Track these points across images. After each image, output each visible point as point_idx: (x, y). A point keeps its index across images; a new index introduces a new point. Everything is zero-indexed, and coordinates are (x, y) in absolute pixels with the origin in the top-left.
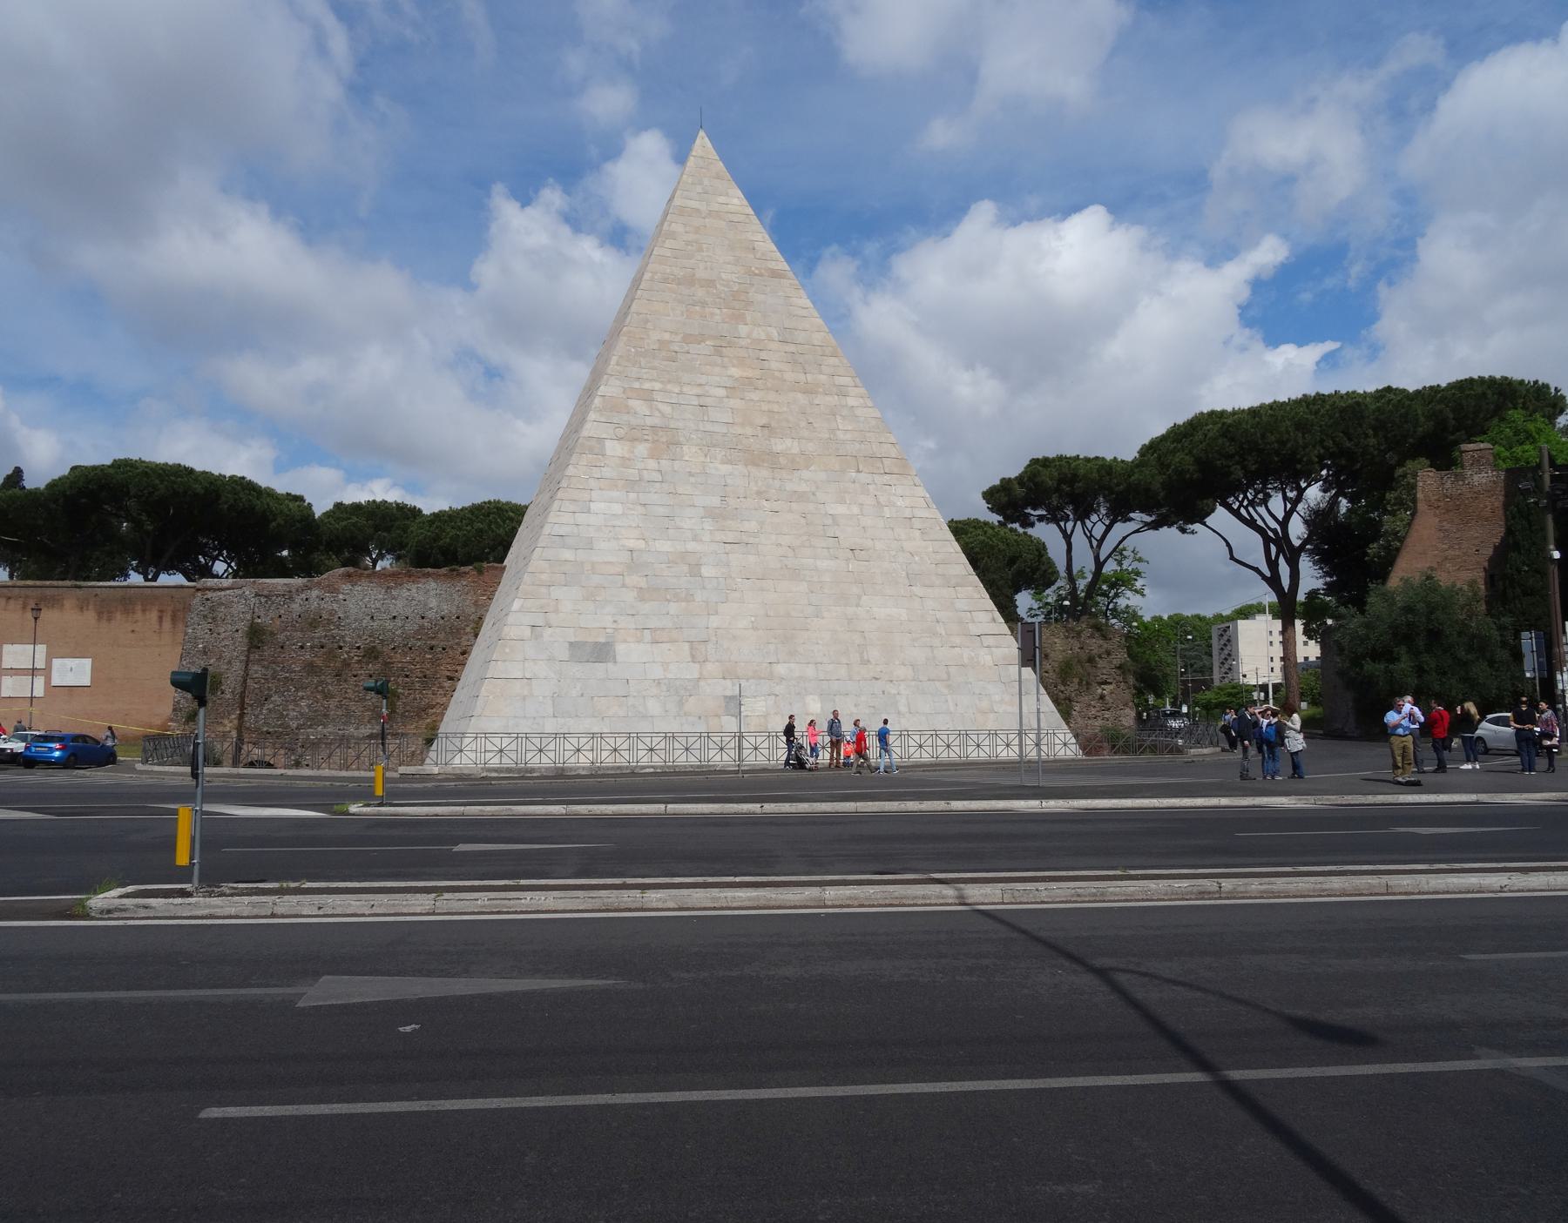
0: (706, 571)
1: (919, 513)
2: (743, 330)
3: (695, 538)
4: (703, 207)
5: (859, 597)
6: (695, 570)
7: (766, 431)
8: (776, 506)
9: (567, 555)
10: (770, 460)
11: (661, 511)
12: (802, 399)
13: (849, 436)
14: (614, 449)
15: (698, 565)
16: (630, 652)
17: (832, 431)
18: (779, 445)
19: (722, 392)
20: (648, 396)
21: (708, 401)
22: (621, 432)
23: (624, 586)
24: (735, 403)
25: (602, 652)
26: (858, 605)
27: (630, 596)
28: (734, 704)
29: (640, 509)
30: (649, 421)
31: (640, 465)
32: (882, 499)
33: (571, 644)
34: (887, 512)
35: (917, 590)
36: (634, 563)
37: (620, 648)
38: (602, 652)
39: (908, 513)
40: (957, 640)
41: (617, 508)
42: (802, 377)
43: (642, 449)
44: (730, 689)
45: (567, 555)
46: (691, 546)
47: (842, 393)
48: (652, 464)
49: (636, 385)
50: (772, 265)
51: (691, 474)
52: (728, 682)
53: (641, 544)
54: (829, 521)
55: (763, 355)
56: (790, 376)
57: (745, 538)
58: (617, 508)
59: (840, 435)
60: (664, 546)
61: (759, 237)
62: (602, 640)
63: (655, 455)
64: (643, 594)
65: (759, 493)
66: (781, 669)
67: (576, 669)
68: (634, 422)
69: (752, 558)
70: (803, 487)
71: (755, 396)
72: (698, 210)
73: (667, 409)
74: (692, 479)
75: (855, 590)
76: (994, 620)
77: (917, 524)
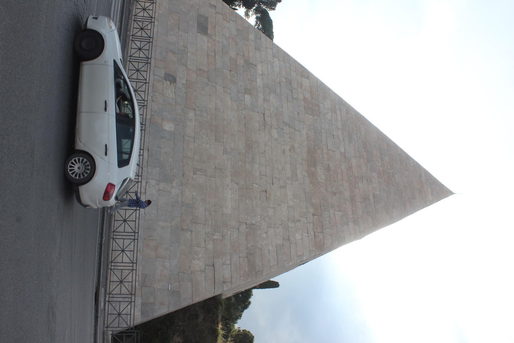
0: (248, 98)
3: (265, 100)
5: (237, 184)
6: (247, 91)
11: (278, 90)
12: (347, 194)
13: (332, 216)
15: (250, 94)
16: (203, 41)
18: (320, 171)
19: (342, 150)
23: (238, 54)
25: (203, 28)
26: (232, 181)
27: (232, 53)
28: (171, 78)
29: (278, 80)
30: (321, 105)
33: (207, 18)
34: (291, 225)
35: (243, 228)
36: (249, 65)
37: (205, 38)
38: (203, 28)
40: (210, 246)
41: (277, 70)
43: (308, 95)
44: (181, 81)
46: (261, 96)
48: (301, 97)
49: (337, 107)
51: (298, 114)
52: (184, 82)
55: (365, 181)
58: (277, 70)
59: (332, 211)
60: (259, 82)
62: (209, 32)
66: (191, 114)
70: (300, 176)
74: (296, 113)
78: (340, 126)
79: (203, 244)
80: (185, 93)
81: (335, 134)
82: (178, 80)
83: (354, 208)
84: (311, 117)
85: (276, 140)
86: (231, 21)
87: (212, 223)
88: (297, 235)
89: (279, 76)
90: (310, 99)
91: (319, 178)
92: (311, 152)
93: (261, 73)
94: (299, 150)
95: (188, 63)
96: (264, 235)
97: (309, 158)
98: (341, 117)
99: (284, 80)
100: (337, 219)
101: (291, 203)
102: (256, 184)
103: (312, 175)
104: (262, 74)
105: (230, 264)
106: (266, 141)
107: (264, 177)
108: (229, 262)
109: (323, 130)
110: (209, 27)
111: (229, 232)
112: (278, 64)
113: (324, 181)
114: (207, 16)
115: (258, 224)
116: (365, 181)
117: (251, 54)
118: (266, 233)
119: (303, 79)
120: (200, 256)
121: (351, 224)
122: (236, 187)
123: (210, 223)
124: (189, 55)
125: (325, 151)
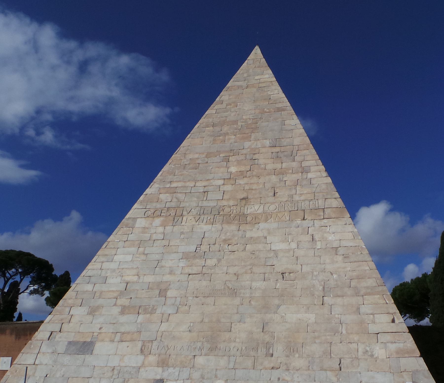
1: (344, 243)
2: (247, 144)
3: (171, 272)
4: (244, 84)
5: (279, 306)
7: (244, 202)
8: (235, 248)
9: (89, 287)
10: (242, 219)
12: (274, 179)
13: (303, 198)
14: (141, 223)
15: (166, 290)
17: (291, 196)
19: (221, 182)
20: (173, 191)
21: (210, 188)
22: (149, 213)
23: (115, 305)
24: (228, 188)
26: (275, 312)
29: (143, 257)
30: (168, 205)
31: (153, 231)
32: (316, 237)
33: (70, 343)
34: (319, 245)
39: (335, 245)
42: (278, 166)
43: (158, 221)
45: (89, 287)
46: (167, 278)
47: (305, 170)
48: (161, 229)
49: (168, 186)
50: (280, 105)
51: (182, 233)
53: (135, 278)
54: (272, 254)
55: (256, 157)
56: (270, 167)
57: (205, 270)
59: (296, 198)
61: (276, 92)
63: (164, 225)
64: (124, 311)
65: (225, 241)
67: (66, 359)
68: (158, 206)
69: (204, 283)
71: (242, 182)
72: (241, 86)
73: (181, 196)
74: (182, 236)
75: (276, 302)
76: (393, 321)
77: (341, 251)
78: (192, 184)
79: (354, 346)
80: (174, 368)
81: (202, 191)
82: (158, 377)
83: (291, 171)
84: (185, 218)
85: (219, 260)
86: (71, 313)
87: (328, 335)
88: (330, 238)
89: (138, 256)
90: (162, 219)
91: (258, 212)
92: (228, 219)
93: (137, 277)
94: (228, 234)
95: (134, 365)
96: (335, 276)
97: (236, 222)
98: (180, 181)
99: (141, 249)
100: (305, 192)
101: (294, 245)
102: (276, 285)
103: (256, 220)
104: (138, 275)
105: (373, 314)
106: (223, 273)
107: (266, 275)
108: (372, 316)
109: (200, 205)
110: (82, 340)
111: (337, 316)
112: (122, 256)
113: (262, 206)
114: (66, 343)
115: (323, 283)
116: (256, 157)
117: (114, 289)
118: (332, 274)
119: (137, 225)
120: (368, 349)
121: (310, 175)
122: (282, 307)
123: (328, 337)
124: (123, 364)
125: (225, 203)
